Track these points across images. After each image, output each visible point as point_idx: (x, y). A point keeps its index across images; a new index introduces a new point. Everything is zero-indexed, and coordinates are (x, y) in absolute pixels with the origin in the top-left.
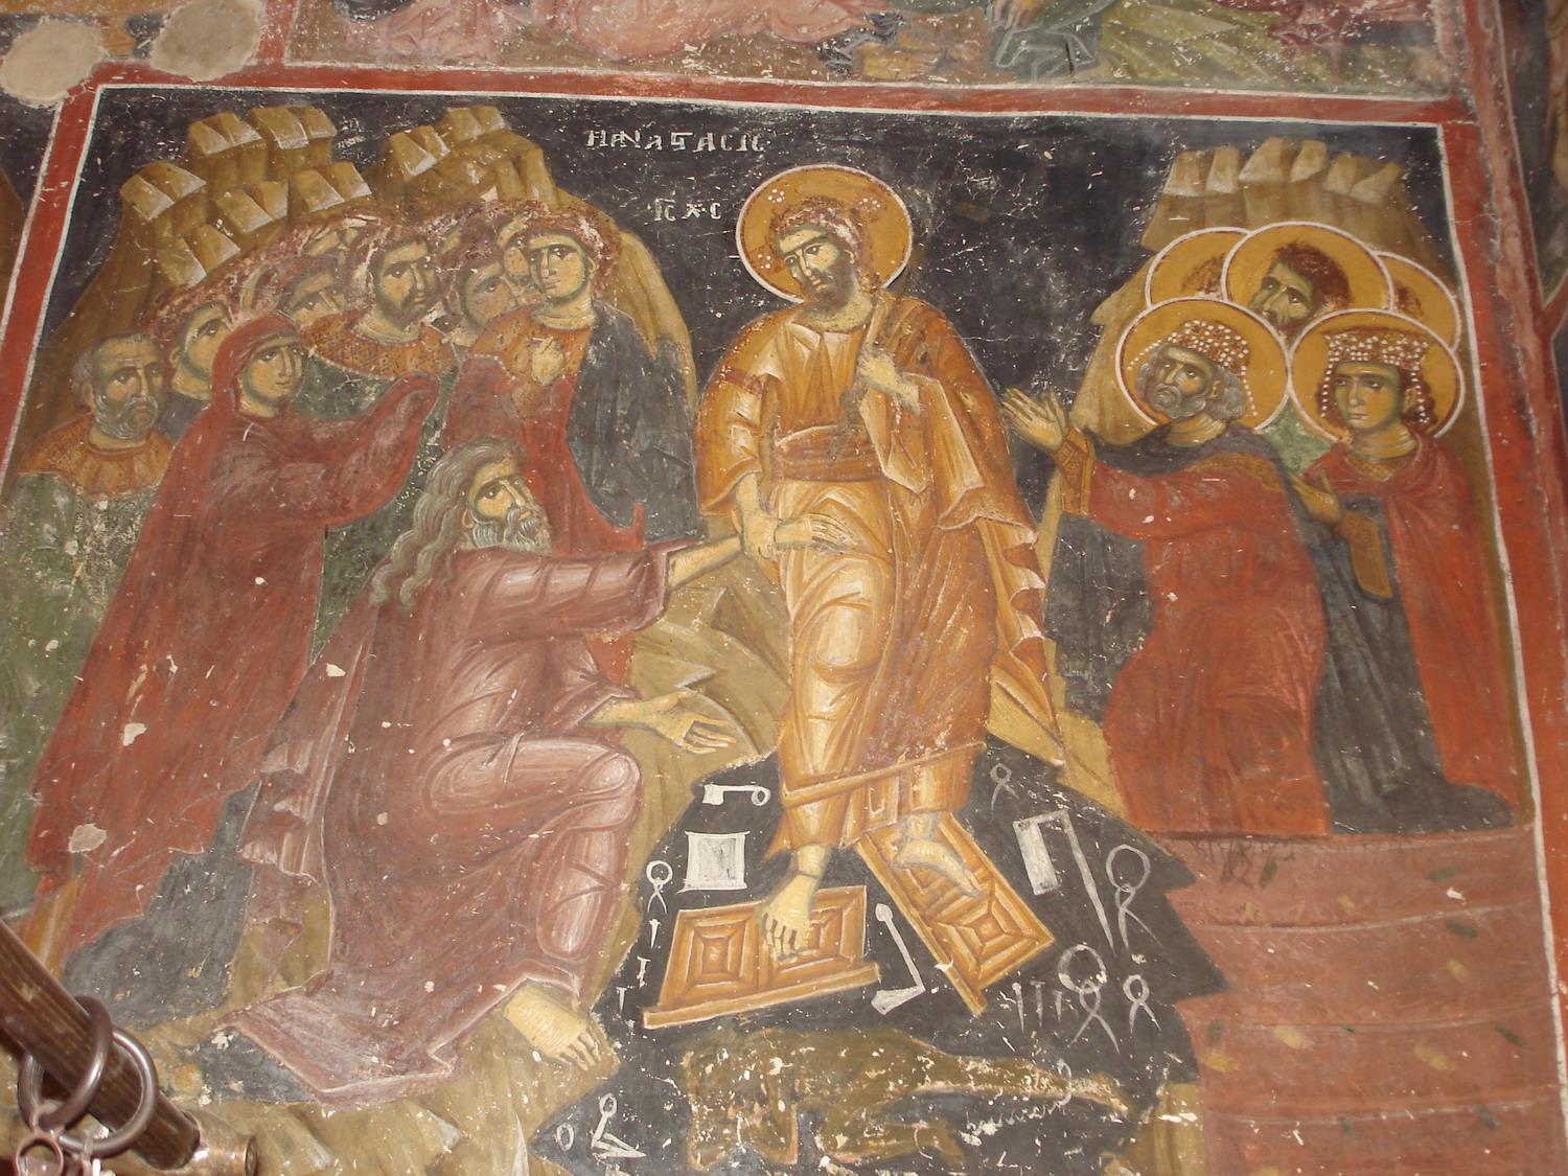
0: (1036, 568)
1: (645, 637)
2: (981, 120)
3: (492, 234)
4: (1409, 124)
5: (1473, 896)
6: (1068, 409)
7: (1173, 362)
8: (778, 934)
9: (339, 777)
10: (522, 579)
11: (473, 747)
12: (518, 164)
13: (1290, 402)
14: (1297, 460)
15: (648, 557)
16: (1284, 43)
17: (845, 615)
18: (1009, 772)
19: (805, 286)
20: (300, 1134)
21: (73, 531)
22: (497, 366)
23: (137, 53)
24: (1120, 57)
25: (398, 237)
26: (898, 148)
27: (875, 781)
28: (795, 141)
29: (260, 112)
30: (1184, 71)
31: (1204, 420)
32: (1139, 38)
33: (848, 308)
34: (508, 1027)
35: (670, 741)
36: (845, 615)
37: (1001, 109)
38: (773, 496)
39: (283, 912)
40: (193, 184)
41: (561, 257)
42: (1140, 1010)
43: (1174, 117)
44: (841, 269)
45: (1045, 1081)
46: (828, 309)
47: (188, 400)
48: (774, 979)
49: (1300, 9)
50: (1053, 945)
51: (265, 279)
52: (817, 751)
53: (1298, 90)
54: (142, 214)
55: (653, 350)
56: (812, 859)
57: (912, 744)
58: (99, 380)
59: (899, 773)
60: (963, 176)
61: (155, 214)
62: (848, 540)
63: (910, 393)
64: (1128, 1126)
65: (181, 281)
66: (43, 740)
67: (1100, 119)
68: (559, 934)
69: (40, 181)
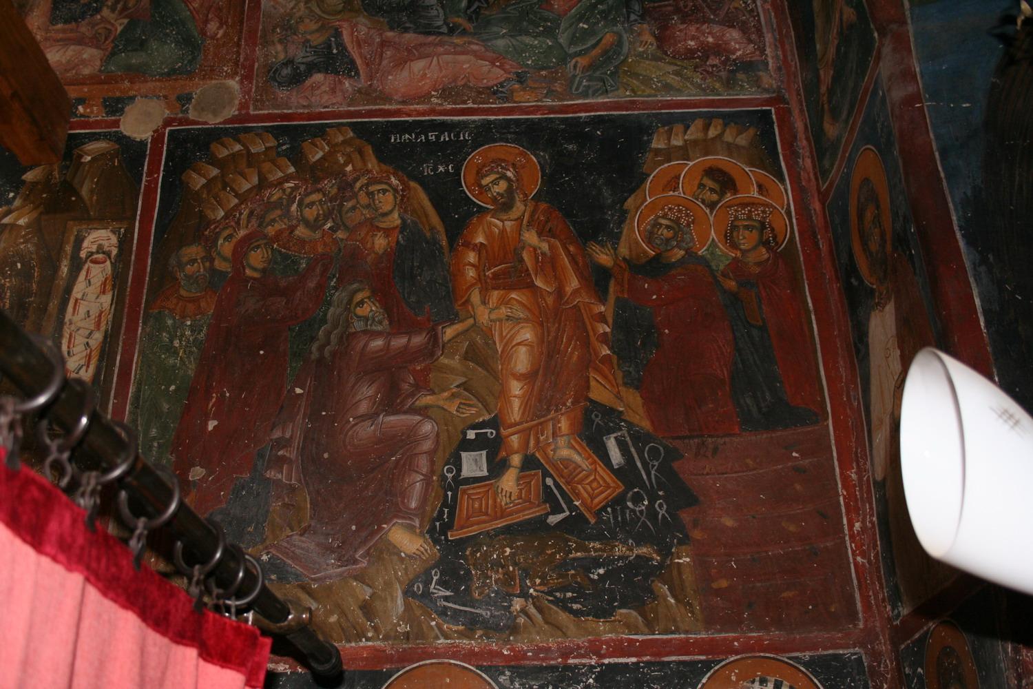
0: (606, 323)
2: (567, 118)
3: (351, 186)
4: (759, 108)
5: (803, 455)
6: (615, 249)
7: (661, 225)
8: (504, 494)
9: (305, 438)
10: (378, 343)
12: (361, 152)
13: (713, 239)
14: (718, 266)
15: (434, 329)
16: (702, 74)
17: (523, 350)
18: (600, 416)
19: (494, 200)
21: (176, 336)
23: (182, 112)
24: (628, 85)
25: (309, 190)
26: (531, 134)
27: (541, 424)
28: (485, 134)
29: (242, 136)
30: (657, 90)
31: (676, 250)
32: (636, 75)
33: (514, 209)
34: (390, 543)
36: (523, 349)
37: (576, 112)
39: (286, 499)
40: (215, 172)
42: (663, 515)
43: (654, 112)
44: (510, 191)
45: (624, 549)
47: (222, 272)
48: (503, 514)
49: (708, 58)
50: (624, 490)
51: (251, 213)
52: (515, 411)
53: (709, 95)
54: (193, 188)
55: (428, 235)
56: (516, 460)
57: (557, 406)
58: (181, 266)
59: (552, 419)
60: (562, 145)
61: (199, 187)
62: (522, 316)
63: (545, 247)
64: (661, 565)
65: (213, 217)
67: (621, 115)
68: (408, 501)
69: (145, 175)
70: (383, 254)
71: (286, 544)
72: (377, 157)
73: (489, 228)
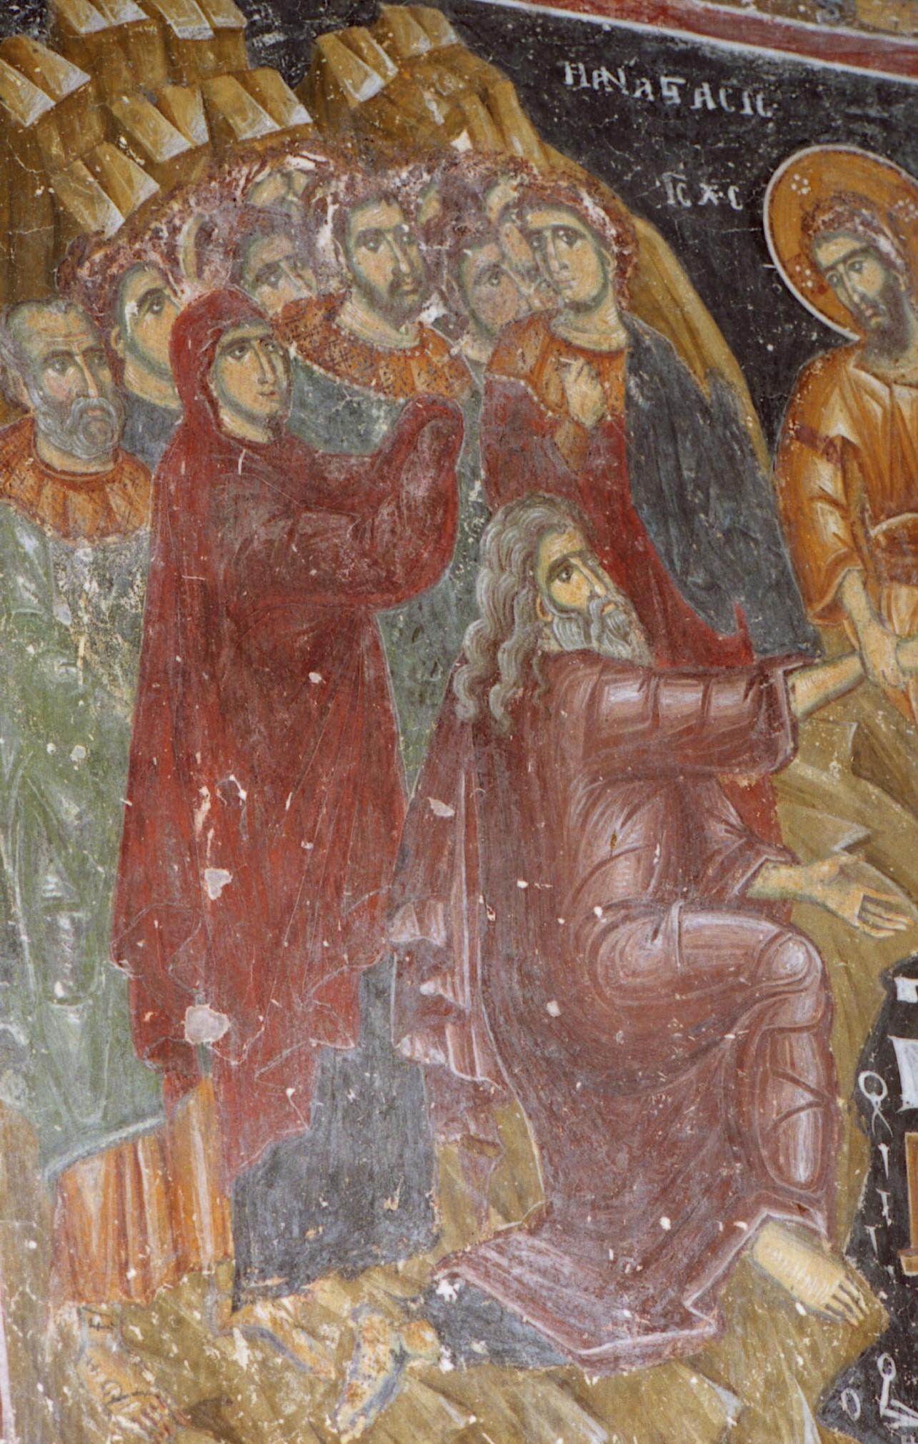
1: (784, 782)
3: (478, 201)
9: (488, 953)
10: (624, 696)
11: (626, 918)
12: (486, 99)
20: (567, 1407)
22: (526, 395)
28: (810, 109)
35: (844, 921)
38: (884, 603)
39: (473, 1128)
40: (73, 78)
41: (570, 244)
46: (889, 352)
47: (153, 408)
51: (205, 234)
54: (15, 116)
55: (705, 389)
61: (31, 119)
65: (95, 228)
66: (107, 887)
70: (596, 428)
71: (492, 1255)
72: (534, 123)
73: (858, 399)
